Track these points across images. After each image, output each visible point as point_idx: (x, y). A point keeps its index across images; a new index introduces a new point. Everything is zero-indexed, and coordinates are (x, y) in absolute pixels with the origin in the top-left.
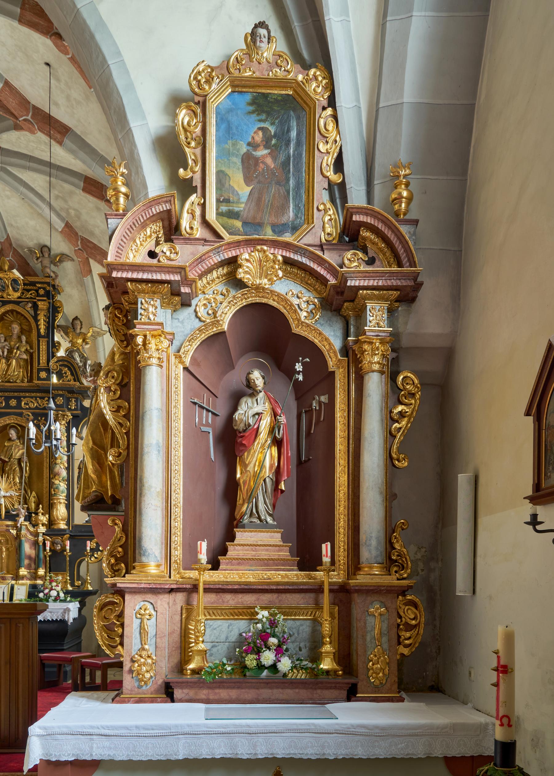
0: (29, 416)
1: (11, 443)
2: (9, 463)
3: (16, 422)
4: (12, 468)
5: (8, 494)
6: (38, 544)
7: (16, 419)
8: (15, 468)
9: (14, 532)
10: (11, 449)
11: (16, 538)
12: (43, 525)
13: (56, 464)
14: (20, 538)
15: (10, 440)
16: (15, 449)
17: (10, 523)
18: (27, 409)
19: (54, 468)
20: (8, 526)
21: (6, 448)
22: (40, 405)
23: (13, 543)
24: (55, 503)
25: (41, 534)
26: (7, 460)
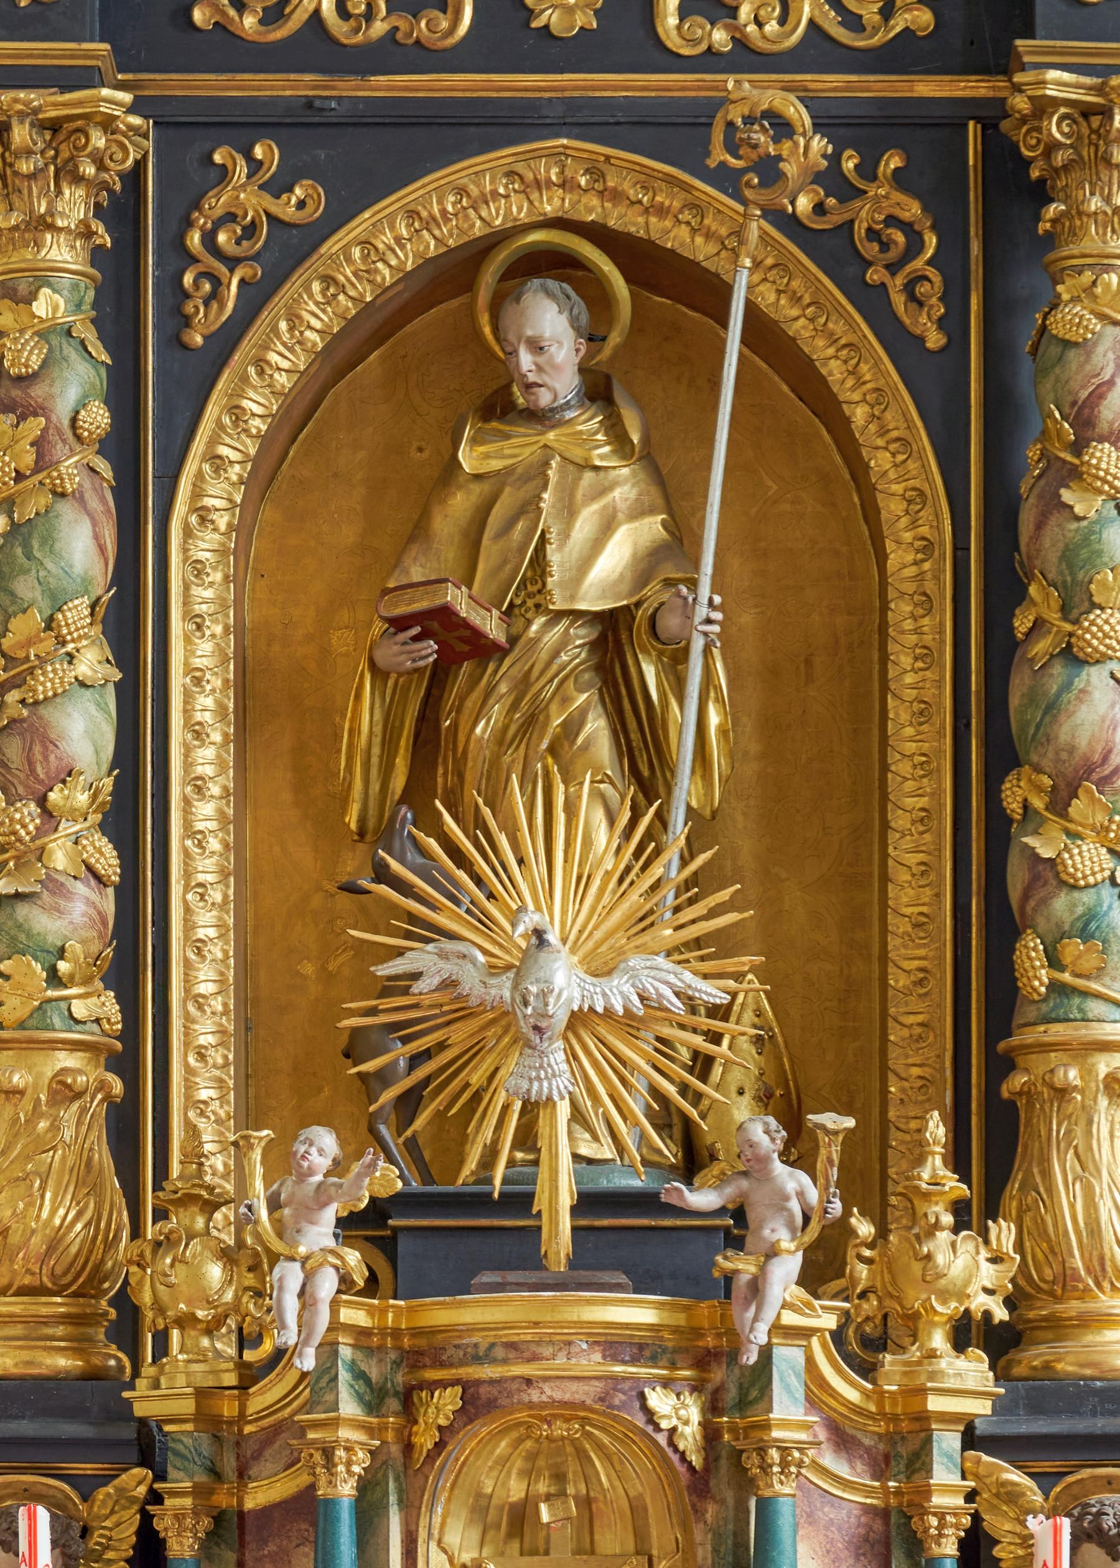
0: (782, 128)
1: (517, 447)
2: (508, 670)
3: (592, 210)
4: (533, 722)
5: (618, 993)
6: (915, 1545)
7: (595, 172)
8: (572, 728)
9: (678, 1412)
10: (530, 507)
11: (700, 1484)
12: (963, 1334)
13: (1072, 656)
14: (745, 1483)
15: (503, 405)
16: (569, 512)
17: (638, 1312)
18: (710, 60)
19: (1052, 708)
20: (616, 1343)
21: (460, 503)
22: (853, 22)
23: (662, 1534)
24: (1062, 1093)
25: (948, 1441)
26: (492, 626)
